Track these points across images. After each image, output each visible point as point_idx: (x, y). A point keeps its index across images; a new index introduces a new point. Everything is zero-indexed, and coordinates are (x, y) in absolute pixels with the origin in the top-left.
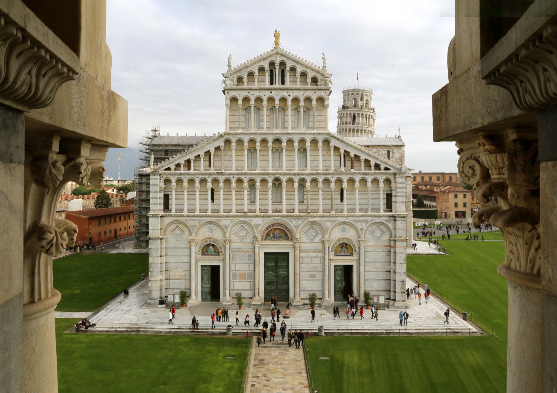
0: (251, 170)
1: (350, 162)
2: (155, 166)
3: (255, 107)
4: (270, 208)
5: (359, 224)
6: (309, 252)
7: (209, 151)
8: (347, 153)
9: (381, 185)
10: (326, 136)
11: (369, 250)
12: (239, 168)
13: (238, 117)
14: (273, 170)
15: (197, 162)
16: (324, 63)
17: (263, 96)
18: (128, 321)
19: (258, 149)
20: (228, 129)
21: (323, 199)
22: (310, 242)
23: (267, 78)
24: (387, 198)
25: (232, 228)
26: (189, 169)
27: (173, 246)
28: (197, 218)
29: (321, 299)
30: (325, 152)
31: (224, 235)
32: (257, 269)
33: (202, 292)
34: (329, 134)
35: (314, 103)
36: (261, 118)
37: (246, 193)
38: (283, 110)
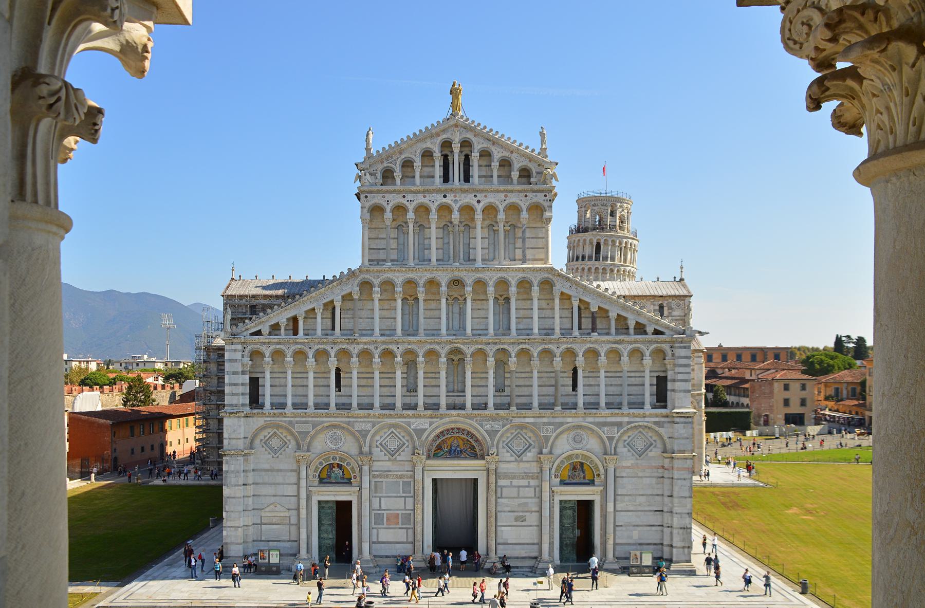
0: (409, 335)
1: (590, 320)
2: (234, 327)
3: (416, 222)
4: (443, 402)
5: (605, 429)
6: (514, 478)
7: (332, 301)
8: (584, 306)
9: (648, 361)
10: (546, 275)
11: (624, 474)
12: (388, 332)
13: (384, 242)
14: (448, 335)
15: (310, 320)
16: (543, 141)
17: (430, 204)
18: (186, 595)
19: (421, 297)
20: (367, 263)
21: (539, 386)
22: (516, 461)
23: (438, 171)
24: (658, 385)
25: (373, 436)
26: (296, 333)
27: (267, 466)
28: (310, 419)
29: (536, 558)
30: (544, 304)
31: (361, 448)
32: (419, 506)
33: (320, 547)
34: (552, 270)
35: (524, 215)
36: (426, 242)
37: (399, 374)
38: (467, 228)
